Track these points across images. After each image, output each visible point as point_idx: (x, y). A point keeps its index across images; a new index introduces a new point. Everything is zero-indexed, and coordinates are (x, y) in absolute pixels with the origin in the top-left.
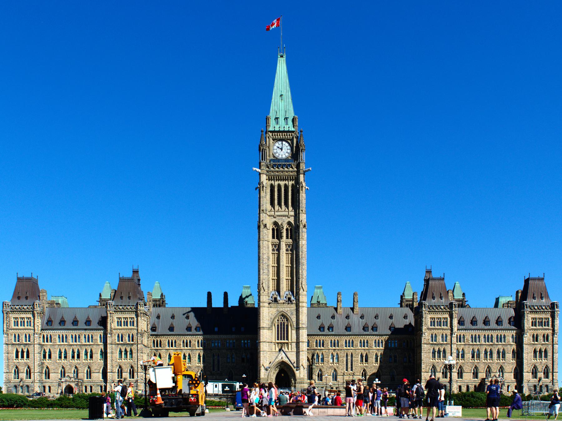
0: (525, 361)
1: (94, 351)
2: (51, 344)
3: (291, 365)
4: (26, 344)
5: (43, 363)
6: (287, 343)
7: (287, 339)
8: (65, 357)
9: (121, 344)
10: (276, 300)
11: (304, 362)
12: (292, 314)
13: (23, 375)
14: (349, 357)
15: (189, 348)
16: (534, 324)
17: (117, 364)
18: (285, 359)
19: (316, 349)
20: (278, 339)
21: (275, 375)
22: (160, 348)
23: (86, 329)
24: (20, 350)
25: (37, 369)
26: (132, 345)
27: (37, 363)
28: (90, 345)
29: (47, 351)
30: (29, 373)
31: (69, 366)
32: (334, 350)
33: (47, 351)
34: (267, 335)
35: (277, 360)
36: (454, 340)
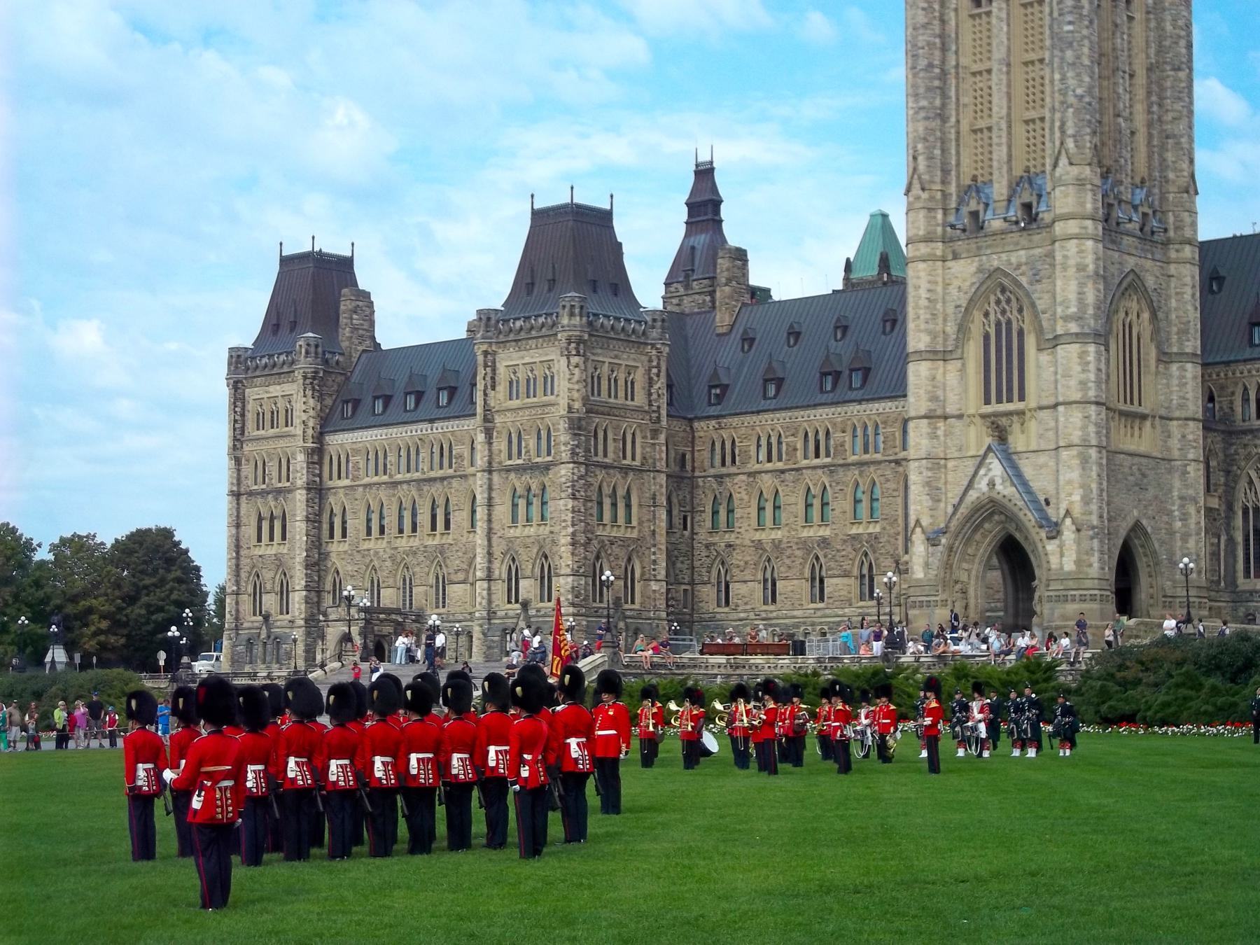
1: (452, 501)
2: (346, 482)
3: (1029, 518)
4: (279, 492)
5: (324, 556)
6: (1021, 413)
7: (1022, 398)
8: (382, 531)
9: (519, 470)
11: (1076, 498)
13: (270, 602)
15: (824, 460)
17: (503, 547)
18: (1006, 490)
20: (987, 402)
22: (733, 470)
23: (432, 421)
24: (265, 513)
25: (299, 580)
26: (547, 467)
28: (442, 479)
29: (338, 510)
30: (284, 592)
31: (389, 563)
33: (338, 510)
34: (940, 382)
35: (973, 495)
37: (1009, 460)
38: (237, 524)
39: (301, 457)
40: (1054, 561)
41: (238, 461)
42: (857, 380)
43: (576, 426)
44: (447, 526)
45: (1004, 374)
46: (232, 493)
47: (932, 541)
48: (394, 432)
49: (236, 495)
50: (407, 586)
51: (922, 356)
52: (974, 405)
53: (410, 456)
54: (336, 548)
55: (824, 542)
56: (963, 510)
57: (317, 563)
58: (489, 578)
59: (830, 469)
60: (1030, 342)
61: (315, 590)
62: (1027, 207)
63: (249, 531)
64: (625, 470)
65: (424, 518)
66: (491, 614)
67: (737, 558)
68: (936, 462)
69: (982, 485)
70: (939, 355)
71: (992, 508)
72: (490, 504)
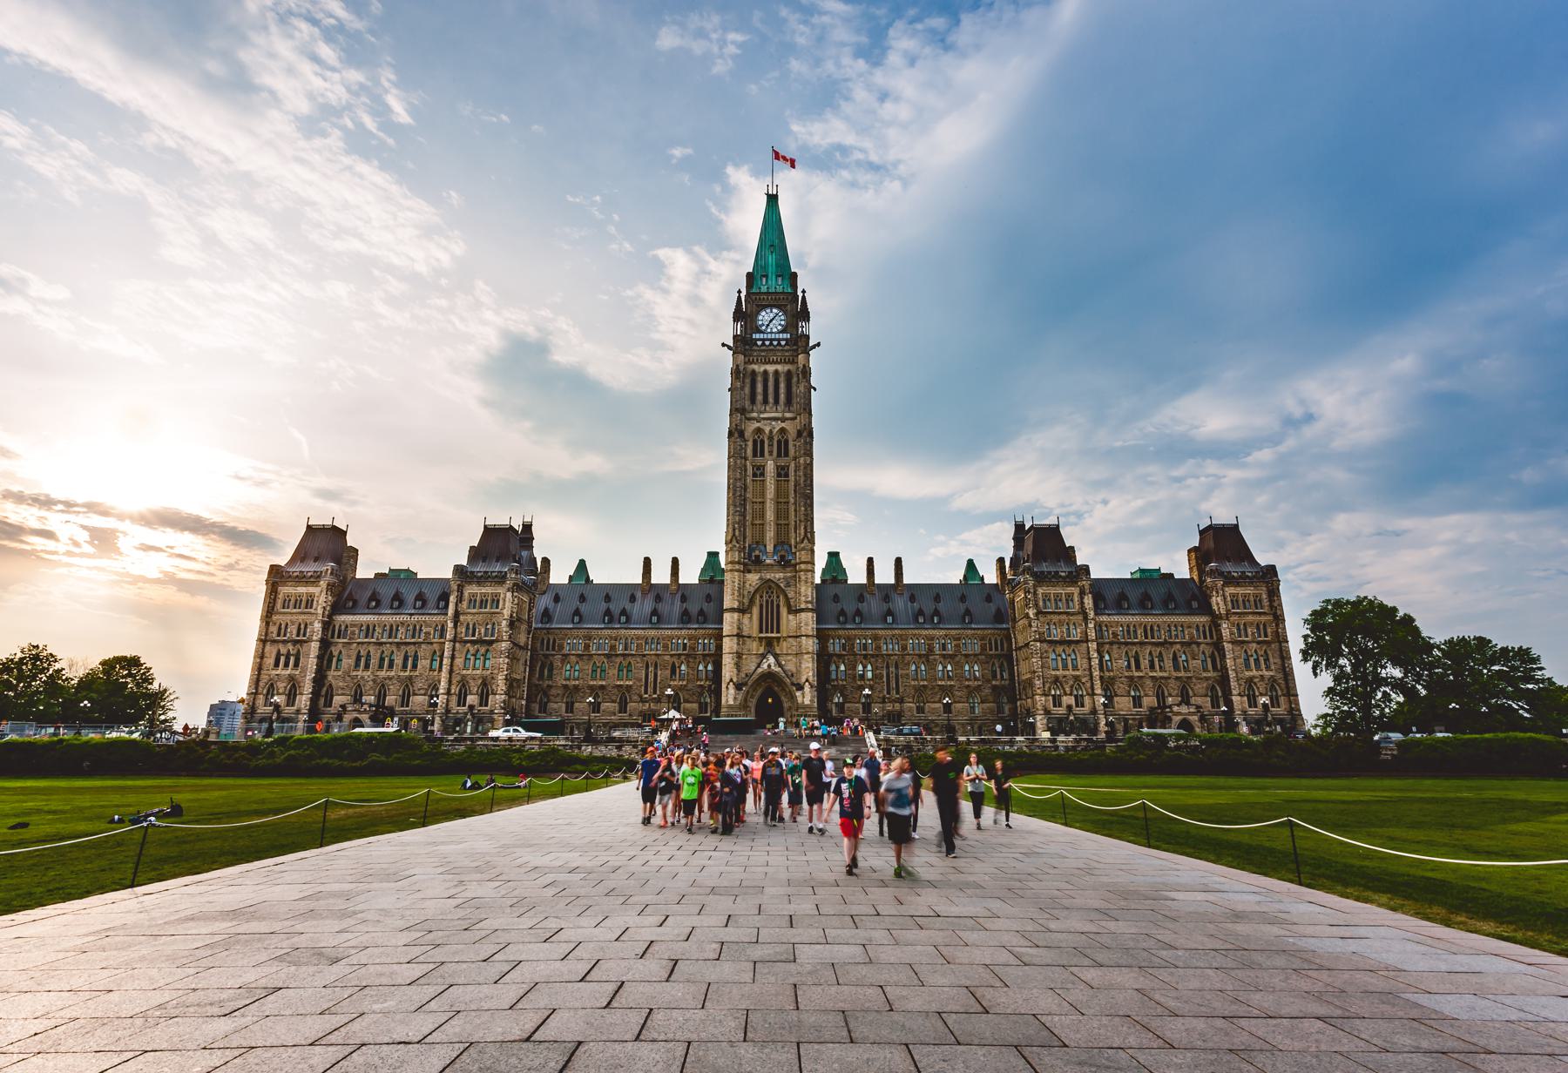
0: (1232, 674)
6: (778, 639)
8: (367, 667)
9: (473, 642)
10: (758, 562)
12: (788, 585)
14: (892, 669)
16: (1235, 603)
18: (776, 669)
19: (831, 656)
21: (754, 701)
24: (283, 651)
25: (307, 688)
26: (491, 643)
27: (310, 675)
29: (336, 653)
30: (292, 697)
32: (865, 656)
36: (1092, 635)
37: (776, 656)
38: (261, 656)
39: (318, 626)
40: (800, 700)
41: (268, 624)
42: (623, 619)
43: (512, 625)
44: (415, 666)
45: (770, 621)
46: (259, 640)
47: (738, 687)
48: (384, 618)
49: (264, 641)
50: (381, 696)
51: (732, 610)
52: (755, 633)
53: (392, 631)
54: (332, 674)
55: (602, 687)
56: (755, 677)
57: (320, 679)
58: (448, 693)
59: (608, 656)
60: (784, 611)
61: (316, 694)
62: (782, 557)
63: (270, 661)
64: (521, 648)
65: (398, 661)
66: (448, 711)
67: (553, 692)
68: (739, 655)
69: (765, 666)
70: (742, 610)
71: (769, 676)
72: (453, 657)
